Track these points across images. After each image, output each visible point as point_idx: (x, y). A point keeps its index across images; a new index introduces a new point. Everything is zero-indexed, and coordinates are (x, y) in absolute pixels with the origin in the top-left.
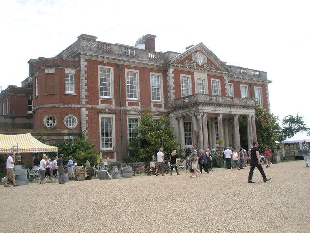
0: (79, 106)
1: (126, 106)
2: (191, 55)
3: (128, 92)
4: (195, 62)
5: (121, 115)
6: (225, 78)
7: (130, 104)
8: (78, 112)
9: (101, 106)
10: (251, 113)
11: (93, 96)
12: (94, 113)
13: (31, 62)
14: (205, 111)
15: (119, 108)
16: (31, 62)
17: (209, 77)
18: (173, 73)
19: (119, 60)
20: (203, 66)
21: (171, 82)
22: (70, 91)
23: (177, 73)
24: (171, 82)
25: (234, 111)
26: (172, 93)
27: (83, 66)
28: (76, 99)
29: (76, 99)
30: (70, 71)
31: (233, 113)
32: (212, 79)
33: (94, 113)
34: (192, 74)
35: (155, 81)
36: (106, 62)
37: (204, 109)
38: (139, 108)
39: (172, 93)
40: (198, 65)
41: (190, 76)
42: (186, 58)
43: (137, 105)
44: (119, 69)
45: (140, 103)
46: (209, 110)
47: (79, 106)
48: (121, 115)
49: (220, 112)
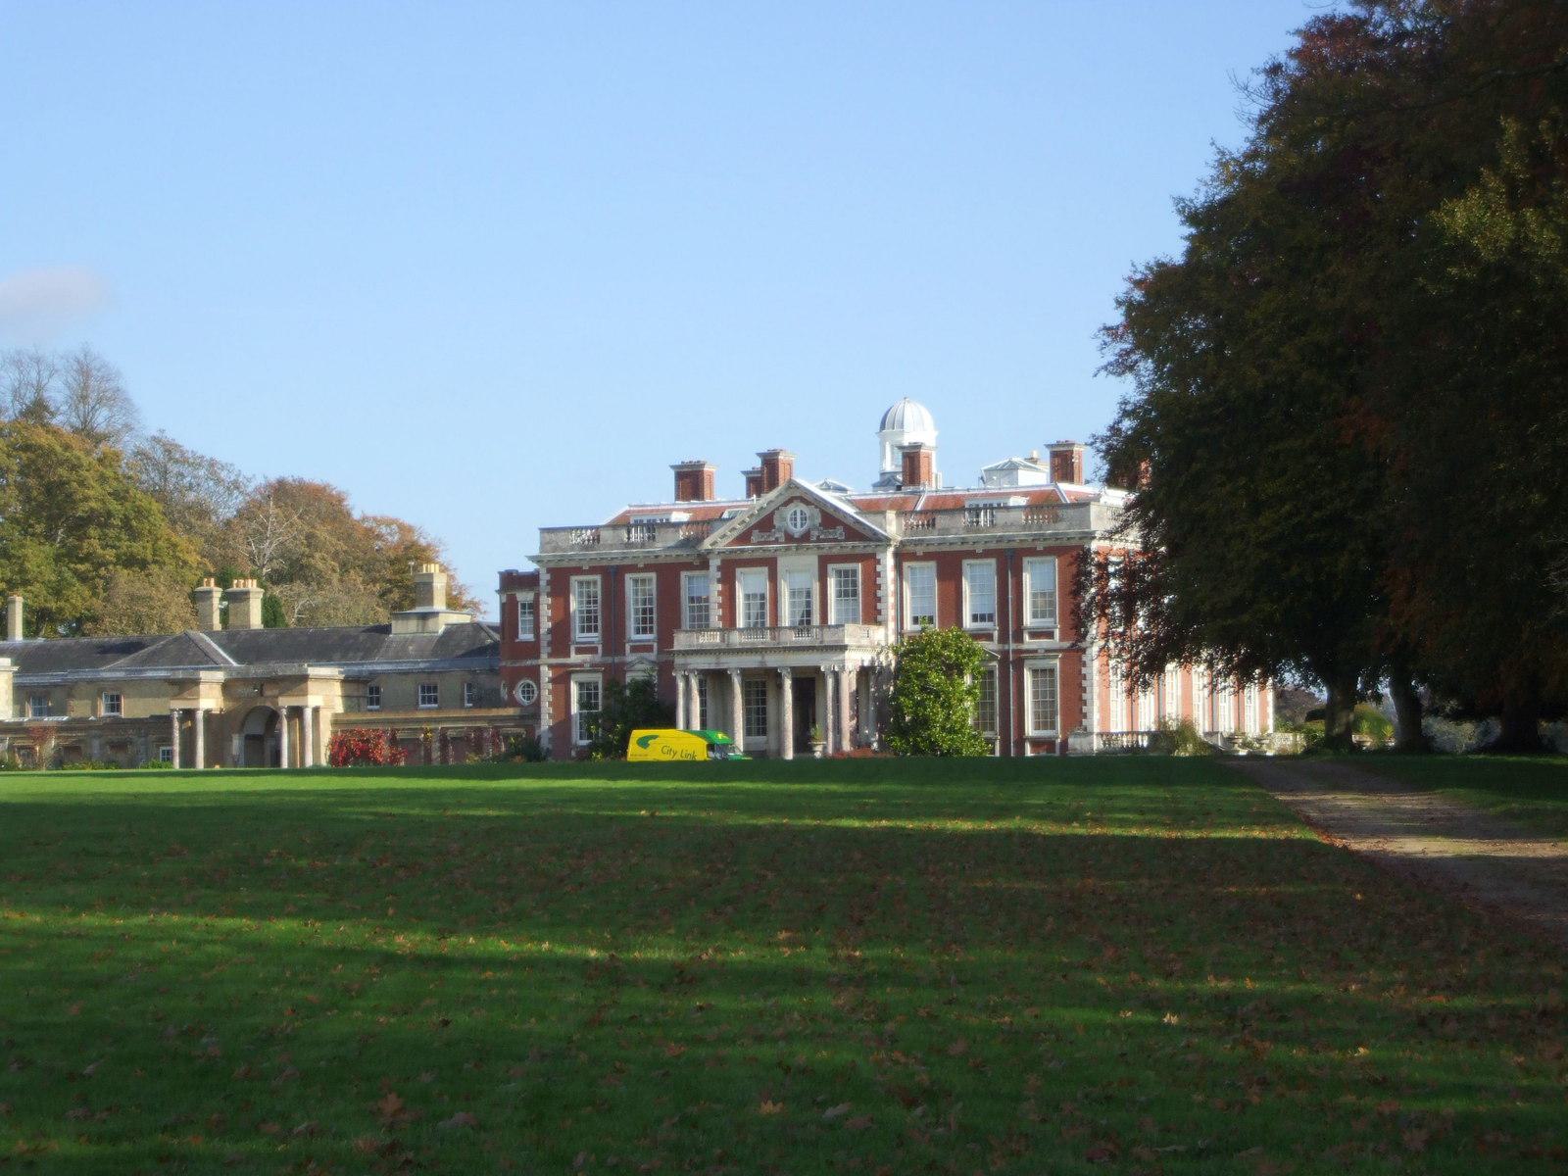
0: (534, 662)
1: (624, 655)
3: (651, 619)
4: (779, 530)
7: (635, 649)
8: (535, 673)
9: (575, 658)
13: (501, 574)
14: (691, 667)
15: (609, 660)
16: (501, 574)
17: (824, 562)
18: (719, 568)
20: (806, 537)
25: (772, 661)
27: (543, 583)
28: (533, 650)
29: (533, 650)
32: (831, 567)
34: (771, 564)
36: (586, 568)
38: (653, 656)
40: (789, 538)
43: (649, 649)
45: (655, 645)
47: (534, 662)
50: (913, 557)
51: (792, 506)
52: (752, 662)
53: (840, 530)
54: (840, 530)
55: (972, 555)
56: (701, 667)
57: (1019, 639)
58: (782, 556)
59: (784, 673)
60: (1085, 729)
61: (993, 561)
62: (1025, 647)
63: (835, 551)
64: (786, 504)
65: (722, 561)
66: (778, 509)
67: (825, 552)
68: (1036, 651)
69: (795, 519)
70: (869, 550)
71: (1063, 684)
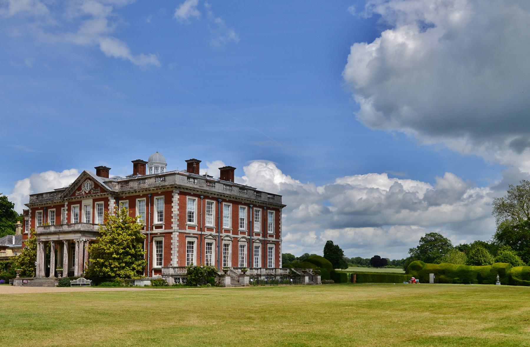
2: (81, 184)
6: (109, 199)
14: (41, 240)
17: (94, 201)
19: (42, 204)
31: (61, 239)
32: (96, 203)
34: (80, 203)
37: (40, 238)
41: (79, 205)
42: (77, 190)
46: (43, 238)
49: (51, 239)
50: (122, 199)
51: (86, 181)
52: (55, 238)
53: (99, 189)
54: (99, 189)
55: (139, 197)
56: (44, 240)
57: (152, 229)
58: (83, 200)
59: (65, 242)
60: (171, 265)
61: (145, 199)
62: (154, 232)
63: (97, 197)
64: (85, 181)
65: (68, 203)
66: (83, 183)
67: (94, 197)
68: (157, 234)
69: (88, 186)
70: (106, 196)
71: (165, 247)
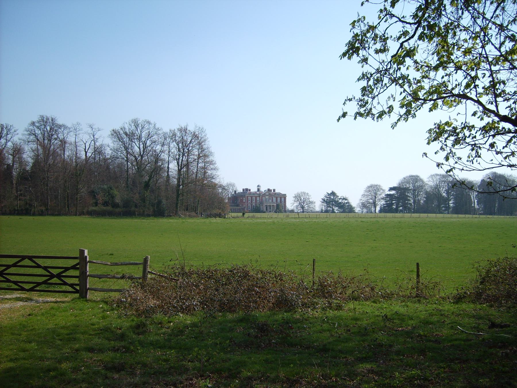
5: (252, 205)
10: (275, 204)
11: (247, 202)
12: (247, 204)
21: (261, 199)
22: (244, 201)
23: (262, 197)
24: (261, 199)
25: (271, 204)
26: (261, 201)
28: (245, 202)
29: (245, 202)
30: (244, 198)
33: (247, 204)
35: (258, 199)
39: (261, 201)
44: (252, 197)
48: (252, 205)
52: (269, 204)
